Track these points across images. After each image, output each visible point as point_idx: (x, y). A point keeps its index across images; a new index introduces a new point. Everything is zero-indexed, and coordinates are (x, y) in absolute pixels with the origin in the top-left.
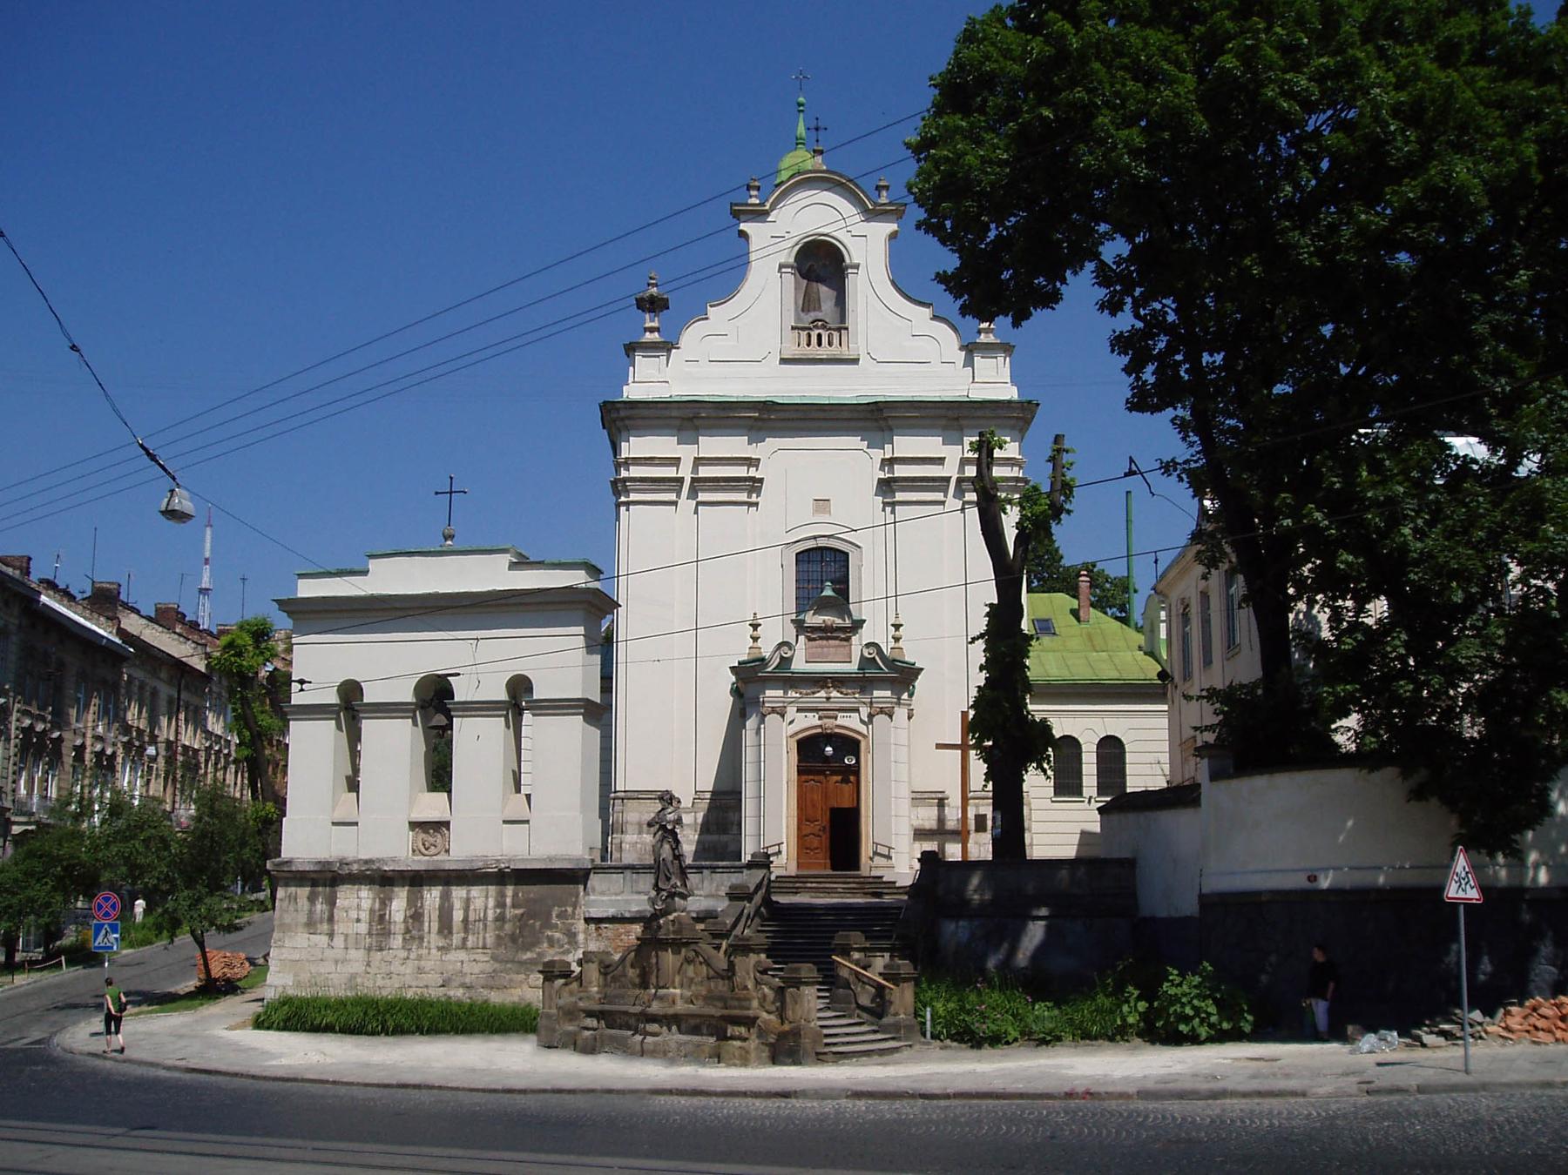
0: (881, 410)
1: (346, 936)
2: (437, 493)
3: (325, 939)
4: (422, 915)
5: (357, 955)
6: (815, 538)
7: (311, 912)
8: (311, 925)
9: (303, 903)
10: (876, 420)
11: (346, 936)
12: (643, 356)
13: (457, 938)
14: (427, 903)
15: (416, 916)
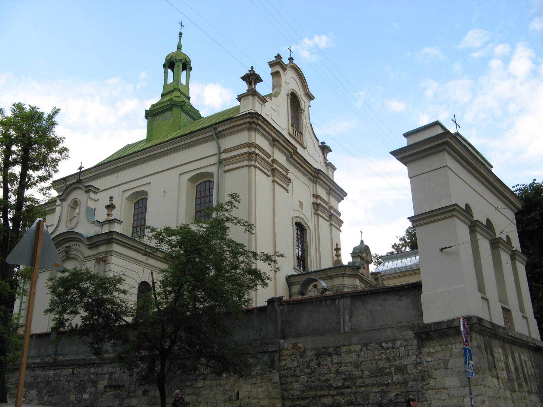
0: (318, 174)
1: (502, 379)
2: (454, 116)
3: (495, 380)
4: (518, 368)
5: (508, 393)
6: (300, 218)
7: (488, 360)
8: (490, 369)
9: (484, 352)
10: (313, 176)
11: (502, 379)
12: (258, 101)
13: (529, 384)
14: (517, 361)
15: (516, 369)
